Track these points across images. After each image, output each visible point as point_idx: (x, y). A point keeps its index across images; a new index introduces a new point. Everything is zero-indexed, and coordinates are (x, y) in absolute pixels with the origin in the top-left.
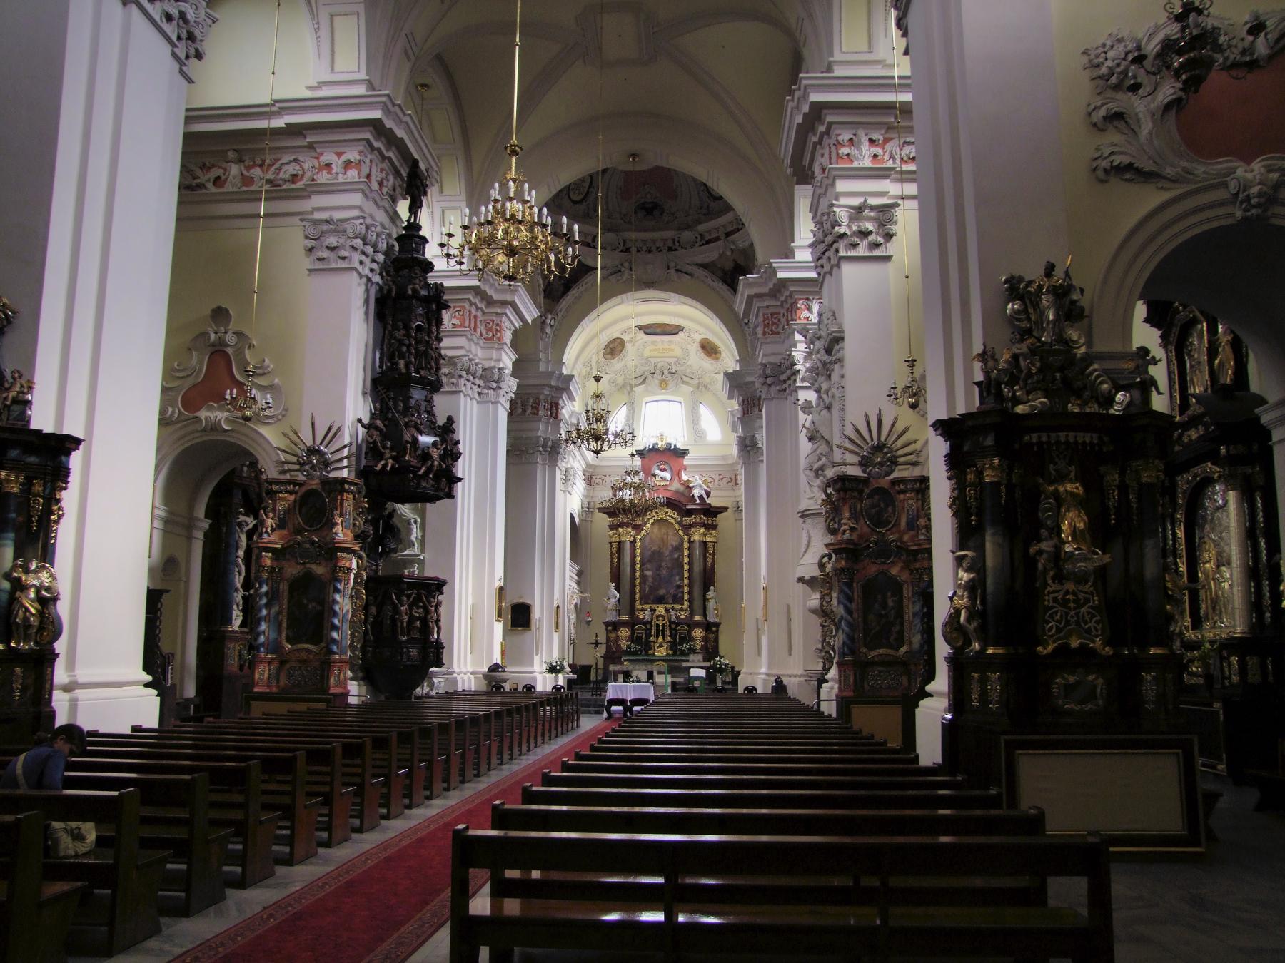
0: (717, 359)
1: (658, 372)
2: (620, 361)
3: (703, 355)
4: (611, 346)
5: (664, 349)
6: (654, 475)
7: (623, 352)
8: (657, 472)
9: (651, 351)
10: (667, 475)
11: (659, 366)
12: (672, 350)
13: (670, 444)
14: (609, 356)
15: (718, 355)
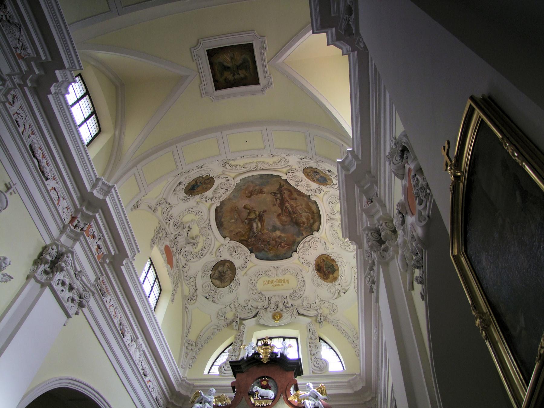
0: (335, 279)
1: (272, 305)
2: (231, 291)
3: (320, 280)
4: (220, 269)
5: (278, 281)
6: (253, 394)
7: (234, 281)
8: (257, 388)
9: (264, 283)
10: (271, 394)
11: (273, 300)
12: (287, 281)
13: (276, 354)
14: (218, 282)
15: (335, 275)
